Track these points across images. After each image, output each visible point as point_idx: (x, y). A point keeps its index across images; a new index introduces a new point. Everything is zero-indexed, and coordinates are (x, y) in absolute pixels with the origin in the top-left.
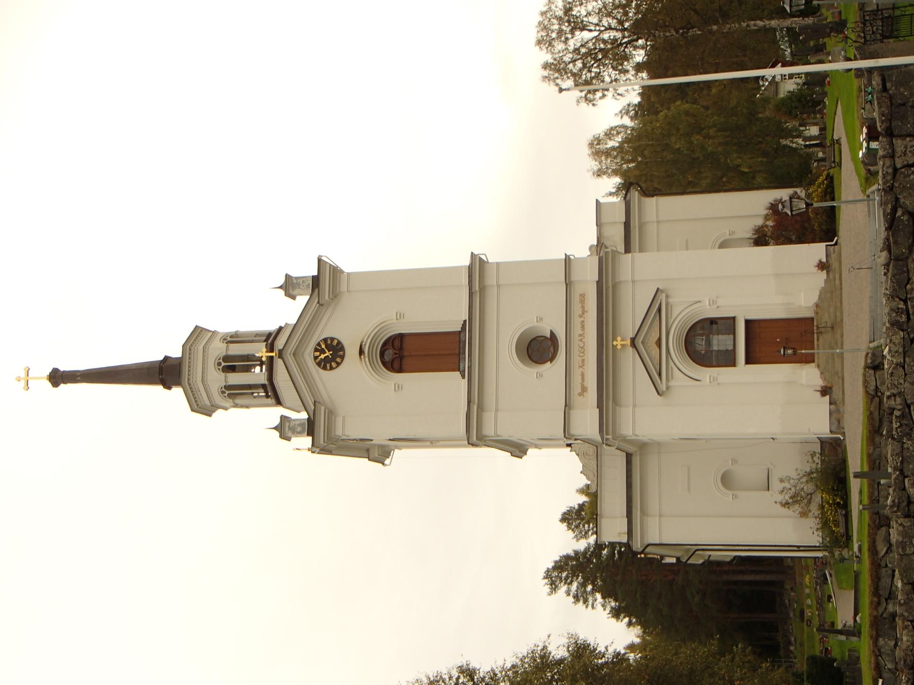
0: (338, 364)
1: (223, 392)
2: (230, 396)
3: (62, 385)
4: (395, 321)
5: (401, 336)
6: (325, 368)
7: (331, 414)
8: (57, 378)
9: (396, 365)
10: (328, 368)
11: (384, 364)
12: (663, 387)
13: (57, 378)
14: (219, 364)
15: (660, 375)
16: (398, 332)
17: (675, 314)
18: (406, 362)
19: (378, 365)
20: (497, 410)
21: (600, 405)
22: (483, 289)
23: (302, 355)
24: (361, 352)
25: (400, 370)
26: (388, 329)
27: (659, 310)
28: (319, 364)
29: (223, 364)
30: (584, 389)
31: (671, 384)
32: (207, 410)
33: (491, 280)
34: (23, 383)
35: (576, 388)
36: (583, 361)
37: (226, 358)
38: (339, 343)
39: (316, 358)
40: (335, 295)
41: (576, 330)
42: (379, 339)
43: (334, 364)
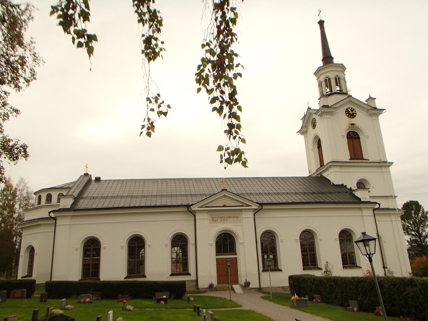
0: (348, 116)
1: (327, 77)
2: (326, 80)
3: (318, 25)
4: (365, 135)
5: (359, 138)
6: (346, 111)
7: (331, 113)
8: (321, 23)
9: (349, 136)
10: (346, 113)
11: (349, 132)
13: (321, 23)
16: (360, 136)
18: (350, 140)
19: (349, 130)
20: (341, 172)
22: (381, 167)
23: (349, 104)
25: (348, 138)
26: (361, 133)
28: (347, 109)
29: (338, 78)
32: (316, 74)
33: (384, 170)
37: (339, 79)
39: (349, 108)
40: (371, 115)
42: (358, 130)
43: (348, 114)
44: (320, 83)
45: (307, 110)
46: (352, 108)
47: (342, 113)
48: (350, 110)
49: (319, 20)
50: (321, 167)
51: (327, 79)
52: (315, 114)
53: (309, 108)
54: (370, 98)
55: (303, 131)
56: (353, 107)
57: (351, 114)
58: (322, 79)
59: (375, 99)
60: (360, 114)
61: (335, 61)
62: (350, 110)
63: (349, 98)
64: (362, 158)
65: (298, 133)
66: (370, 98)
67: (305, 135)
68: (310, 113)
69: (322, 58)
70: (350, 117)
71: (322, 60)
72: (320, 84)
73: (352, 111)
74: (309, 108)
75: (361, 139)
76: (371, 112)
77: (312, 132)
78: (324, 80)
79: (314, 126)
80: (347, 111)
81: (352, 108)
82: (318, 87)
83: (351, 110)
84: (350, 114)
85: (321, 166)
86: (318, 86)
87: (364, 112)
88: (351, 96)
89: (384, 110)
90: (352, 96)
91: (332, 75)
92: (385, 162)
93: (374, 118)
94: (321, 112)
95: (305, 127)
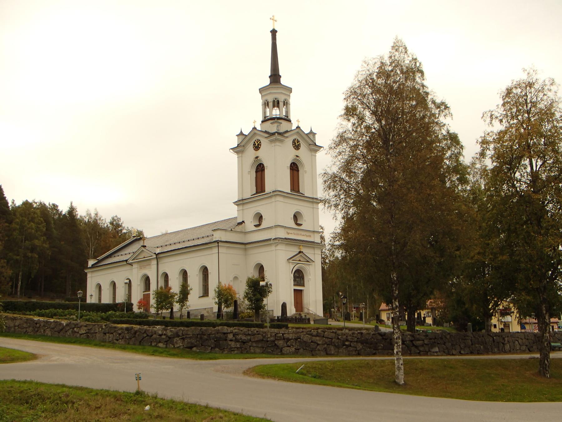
0: (294, 147)
2: (274, 101)
3: (271, 34)
5: (298, 171)
6: (293, 142)
7: (281, 141)
8: (274, 32)
12: (291, 261)
13: (274, 32)
14: (276, 99)
15: (293, 260)
17: (308, 267)
20: (284, 202)
21: (285, 238)
22: (313, 202)
24: (297, 156)
27: (308, 261)
28: (294, 140)
29: (286, 102)
30: (288, 233)
31: (291, 263)
32: (261, 90)
33: (315, 205)
34: (272, 18)
35: (289, 231)
36: (295, 234)
38: (299, 149)
39: (296, 139)
40: (311, 150)
41: (303, 233)
43: (294, 145)
44: (266, 102)
45: (252, 129)
46: (297, 140)
47: (289, 142)
48: (296, 142)
49: (272, 29)
50: (257, 193)
51: (276, 101)
52: (266, 137)
53: (255, 128)
54: (311, 132)
55: (239, 150)
56: (299, 139)
57: (297, 146)
58: (270, 99)
59: (316, 134)
60: (303, 147)
61: (283, 81)
62: (296, 142)
63: (298, 129)
64: (298, 191)
65: (231, 150)
66: (311, 132)
67: (240, 155)
68: (255, 133)
69: (270, 75)
70: (295, 149)
71: (270, 77)
72: (265, 103)
73: (297, 143)
74: (255, 128)
75: (300, 171)
76: (313, 147)
77: (250, 153)
78: (272, 101)
79: (257, 147)
80: (294, 142)
81: (297, 140)
82: (262, 105)
83: (297, 141)
84: (296, 145)
85: (257, 193)
86: (261, 104)
87: (306, 146)
88: (300, 127)
89: (322, 147)
90: (301, 128)
91: (281, 98)
92: (317, 199)
93: (313, 154)
94: (275, 138)
95: (243, 146)
